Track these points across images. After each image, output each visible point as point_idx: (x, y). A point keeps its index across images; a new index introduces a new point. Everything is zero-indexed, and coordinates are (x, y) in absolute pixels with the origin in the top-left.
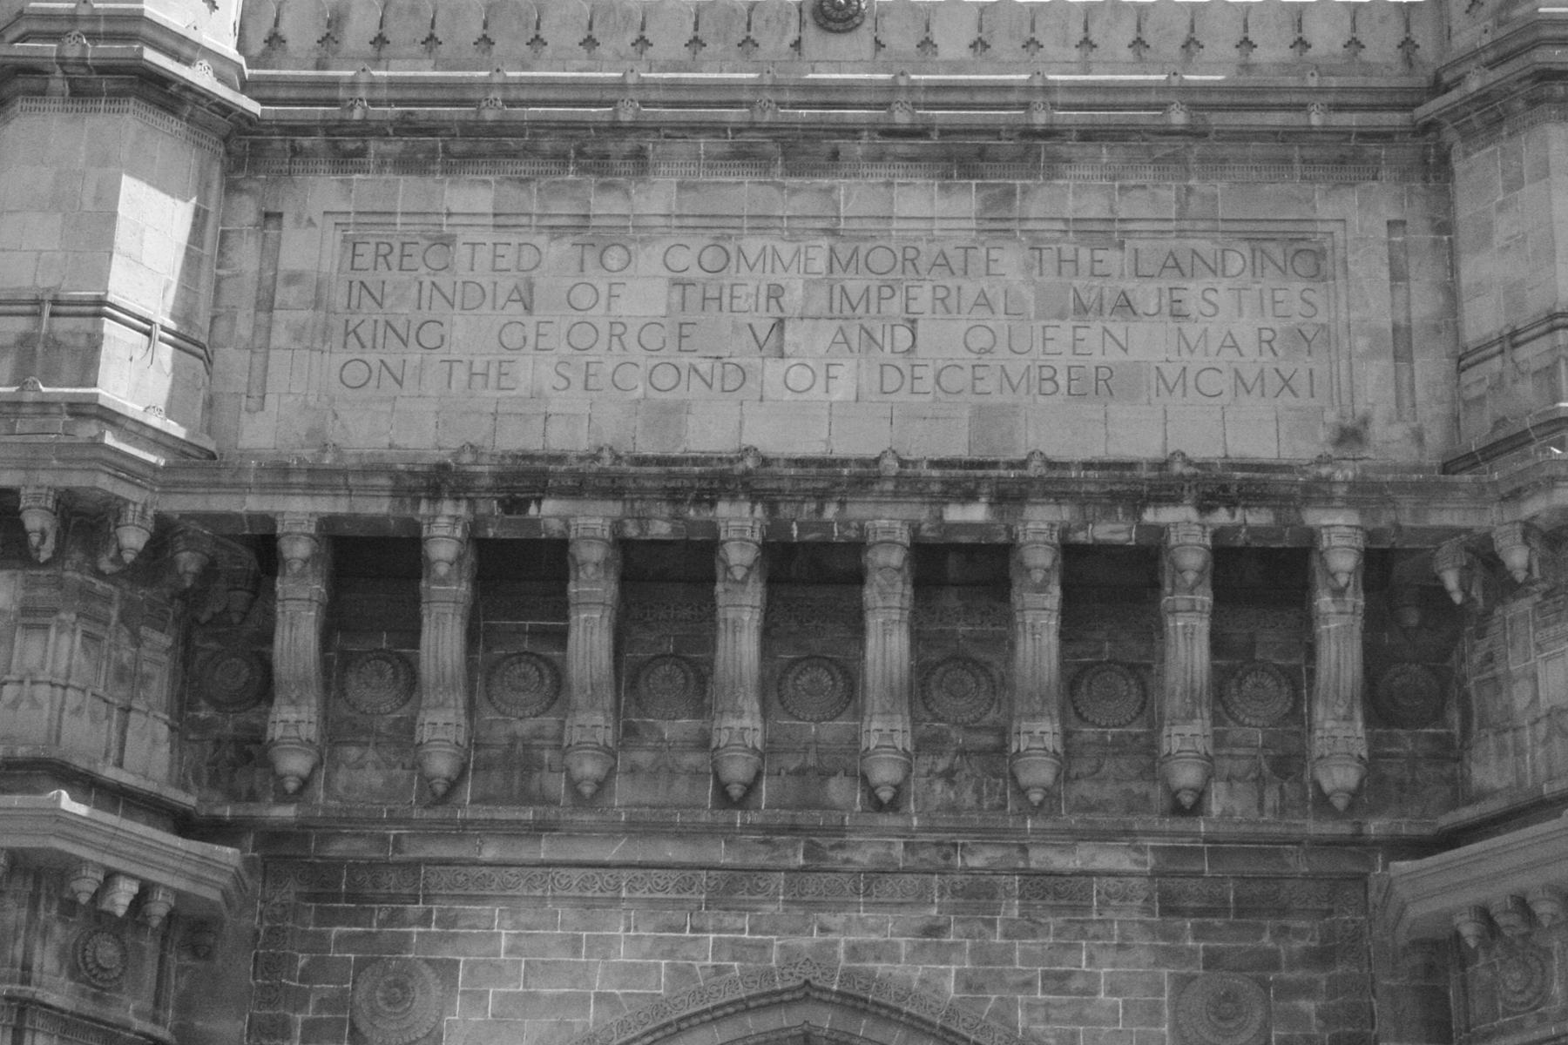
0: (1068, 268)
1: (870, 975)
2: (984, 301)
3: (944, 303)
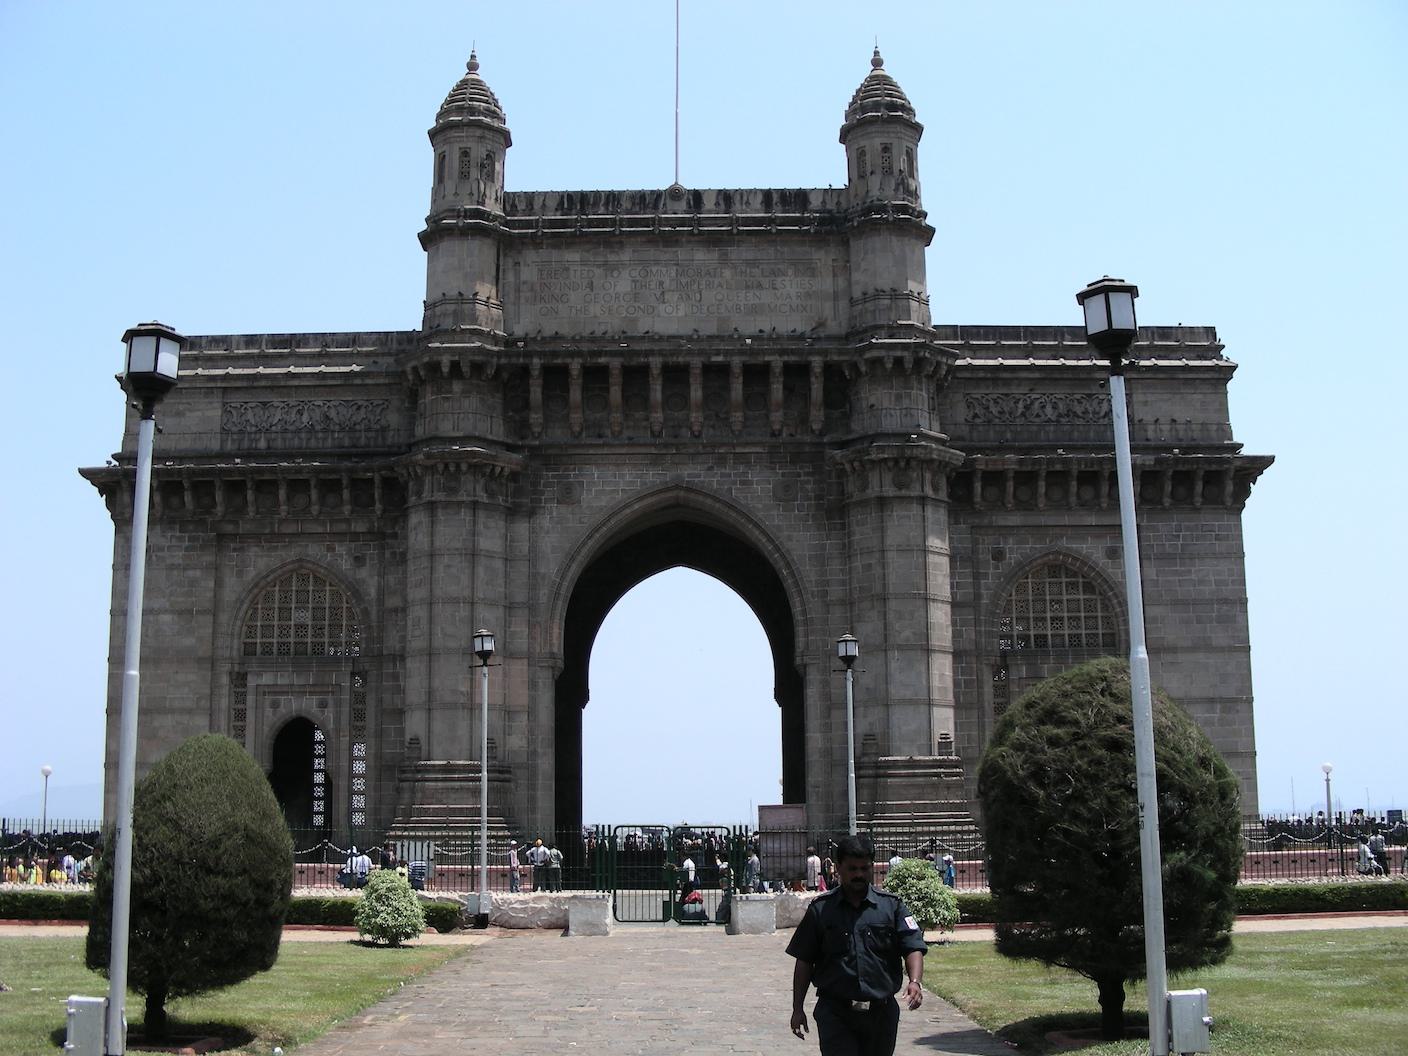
2: (720, 285)
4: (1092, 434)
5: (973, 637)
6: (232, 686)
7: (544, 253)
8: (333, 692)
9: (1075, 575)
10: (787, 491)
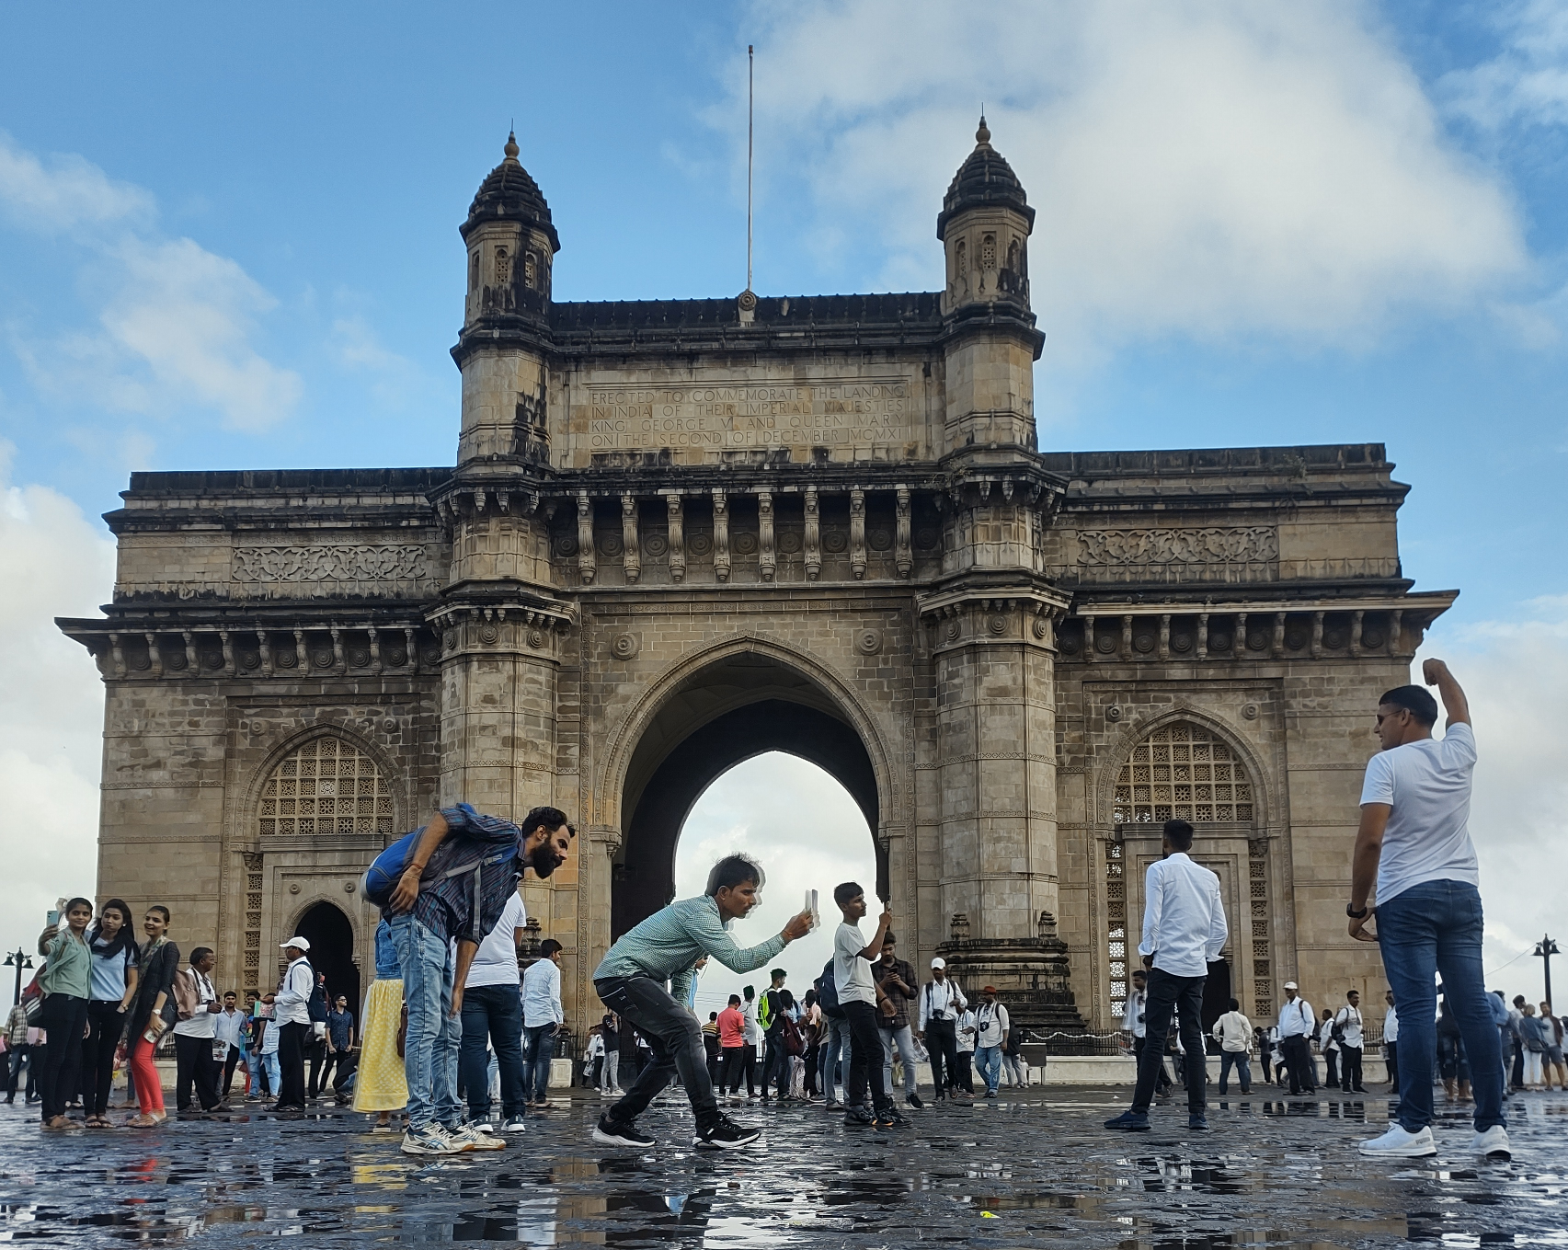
0: (823, 395)
1: (764, 634)
3: (783, 411)
4: (1227, 573)
5: (1083, 809)
6: (247, 869)
7: (600, 376)
9: (1205, 738)
10: (869, 642)
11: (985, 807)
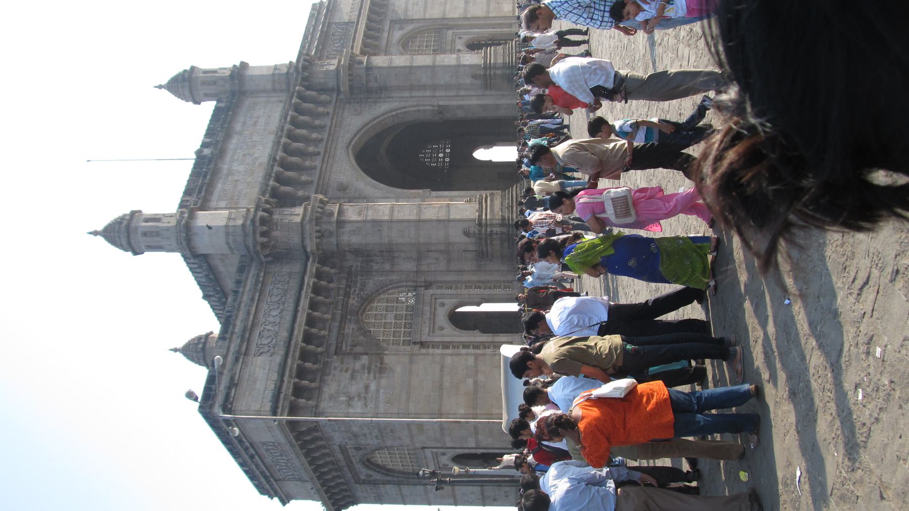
8: (436, 299)
9: (409, 42)
11: (431, 64)
